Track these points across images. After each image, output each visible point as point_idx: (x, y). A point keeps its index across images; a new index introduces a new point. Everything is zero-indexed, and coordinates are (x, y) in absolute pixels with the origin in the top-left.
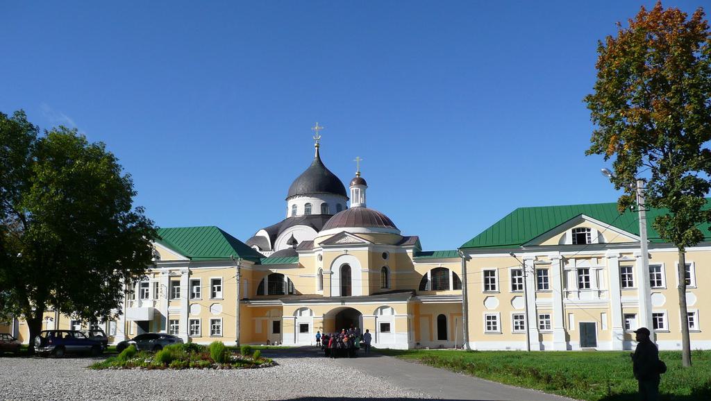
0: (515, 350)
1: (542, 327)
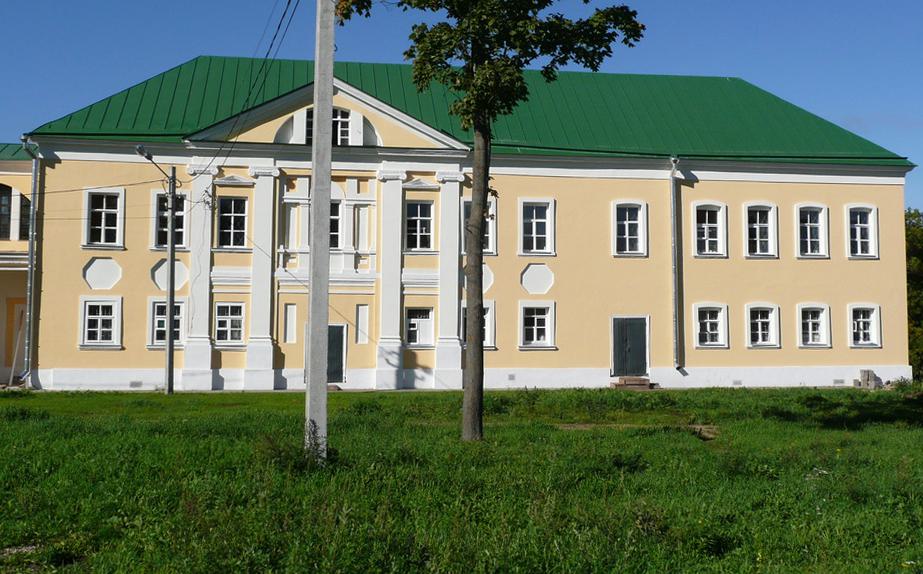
0: (151, 388)
1: (222, 335)
